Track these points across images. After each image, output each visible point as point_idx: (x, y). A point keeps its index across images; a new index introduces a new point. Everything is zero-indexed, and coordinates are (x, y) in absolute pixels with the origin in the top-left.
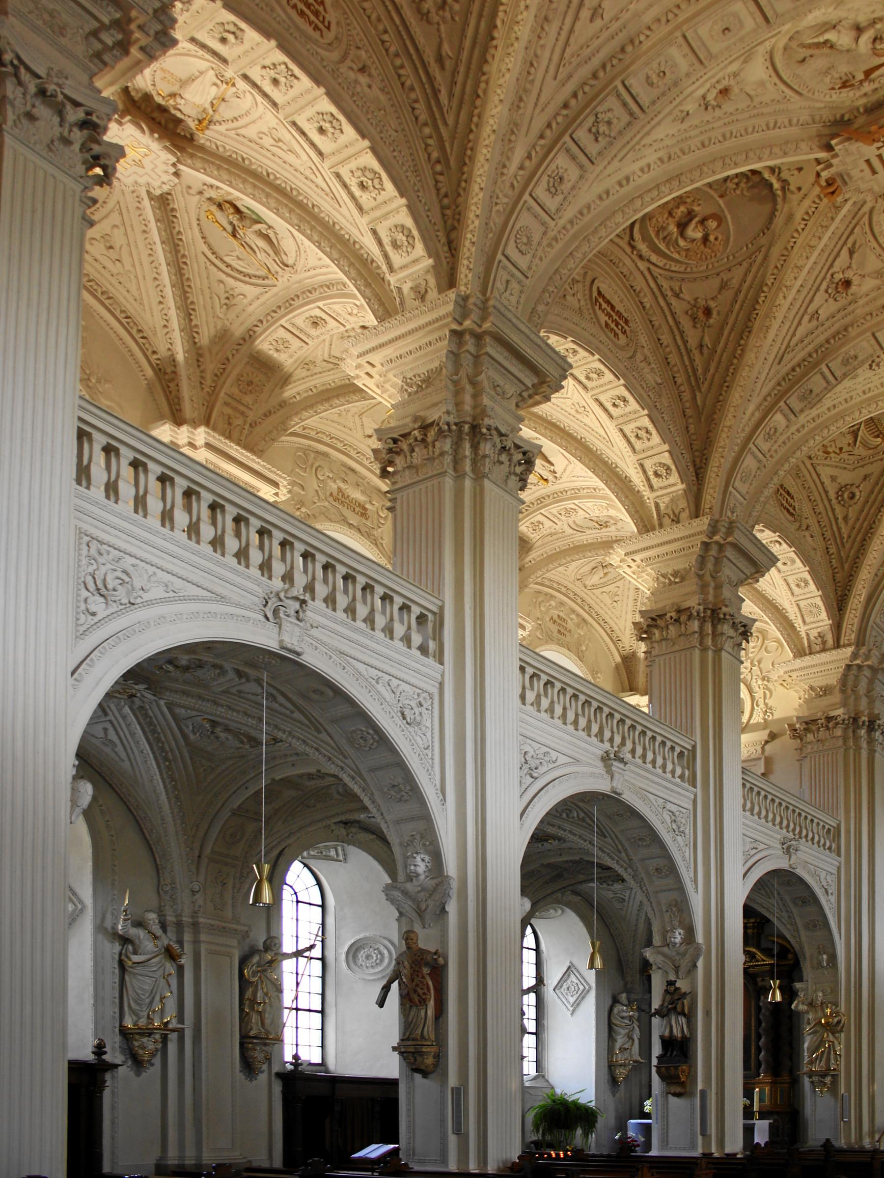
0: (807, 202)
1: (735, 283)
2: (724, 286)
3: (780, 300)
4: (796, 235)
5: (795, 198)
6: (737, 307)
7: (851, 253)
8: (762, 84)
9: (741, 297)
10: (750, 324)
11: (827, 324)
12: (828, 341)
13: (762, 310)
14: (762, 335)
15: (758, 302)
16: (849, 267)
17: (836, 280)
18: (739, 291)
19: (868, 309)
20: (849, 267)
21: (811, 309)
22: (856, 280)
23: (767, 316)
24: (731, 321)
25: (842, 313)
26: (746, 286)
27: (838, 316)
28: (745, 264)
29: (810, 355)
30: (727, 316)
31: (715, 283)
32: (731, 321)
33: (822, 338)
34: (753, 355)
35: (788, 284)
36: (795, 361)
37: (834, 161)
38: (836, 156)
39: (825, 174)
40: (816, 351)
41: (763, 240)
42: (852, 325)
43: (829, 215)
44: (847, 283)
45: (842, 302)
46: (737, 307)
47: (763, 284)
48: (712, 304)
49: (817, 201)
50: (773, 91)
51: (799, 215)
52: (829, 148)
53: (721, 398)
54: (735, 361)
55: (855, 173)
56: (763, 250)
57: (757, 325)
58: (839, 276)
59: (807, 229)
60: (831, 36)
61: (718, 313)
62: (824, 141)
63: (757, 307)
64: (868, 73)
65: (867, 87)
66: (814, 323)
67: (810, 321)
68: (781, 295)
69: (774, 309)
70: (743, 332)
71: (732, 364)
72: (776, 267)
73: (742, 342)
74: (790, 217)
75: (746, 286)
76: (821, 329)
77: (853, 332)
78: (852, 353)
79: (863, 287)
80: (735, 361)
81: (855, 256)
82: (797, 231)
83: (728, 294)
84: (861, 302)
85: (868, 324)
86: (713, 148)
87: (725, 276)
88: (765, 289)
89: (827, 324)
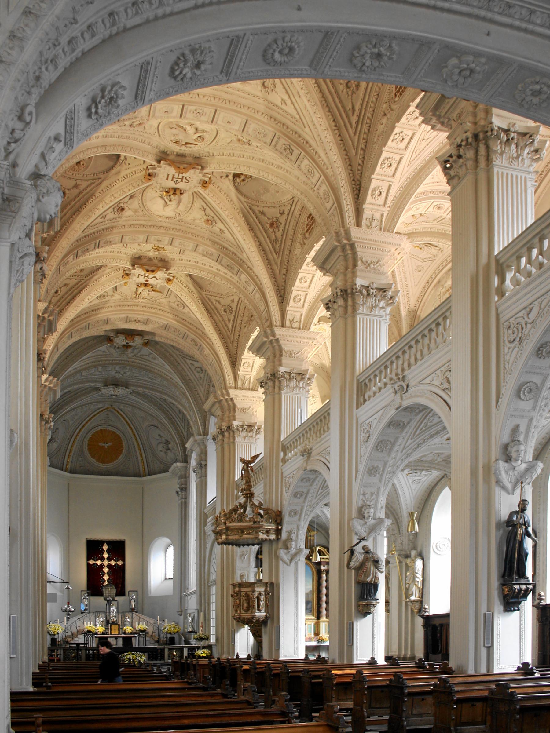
0: (128, 171)
1: (82, 188)
2: (76, 186)
3: (100, 207)
4: (118, 182)
5: (124, 166)
6: (77, 199)
7: (131, 198)
8: (151, 126)
9: (81, 196)
10: (80, 210)
11: (107, 222)
12: (103, 230)
13: (89, 206)
14: (86, 219)
15: (88, 201)
16: (126, 203)
17: (120, 206)
18: (81, 192)
19: (124, 223)
20: (126, 203)
21: (104, 214)
22: (126, 209)
23: (91, 211)
24: (73, 203)
25: (114, 220)
26: (85, 192)
27: (112, 221)
28: (90, 182)
29: (94, 233)
30: (71, 201)
31: (73, 183)
32: (73, 203)
33: (102, 227)
34: (78, 227)
35: (106, 201)
36: (88, 233)
37: (158, 169)
38: (160, 167)
39: (151, 171)
40: (97, 233)
41: (102, 176)
42: (115, 227)
43: (138, 183)
44: (123, 209)
45: (116, 216)
46: (77, 199)
47: (93, 195)
48: (67, 192)
49: (134, 173)
50: (154, 130)
51: (123, 173)
52: (159, 162)
53: (56, 239)
54: (68, 224)
55: (161, 176)
56: (101, 180)
57: (84, 212)
58: (121, 205)
59: (123, 182)
60: (188, 128)
61: (68, 197)
62: (158, 158)
63: (87, 204)
64: (187, 143)
65: (183, 148)
66: (102, 220)
67: (101, 218)
68: (101, 205)
69: (96, 210)
70: (76, 212)
71: (65, 225)
72: (102, 190)
73: (74, 216)
74: (118, 173)
75: (85, 192)
76: (103, 223)
77: (115, 231)
78: (110, 240)
79: (128, 213)
80: (68, 224)
81: (131, 199)
82: (119, 180)
83: (76, 191)
84: (123, 219)
85: (122, 230)
86: (121, 140)
87: (79, 182)
88: (94, 197)
89: (107, 222)
